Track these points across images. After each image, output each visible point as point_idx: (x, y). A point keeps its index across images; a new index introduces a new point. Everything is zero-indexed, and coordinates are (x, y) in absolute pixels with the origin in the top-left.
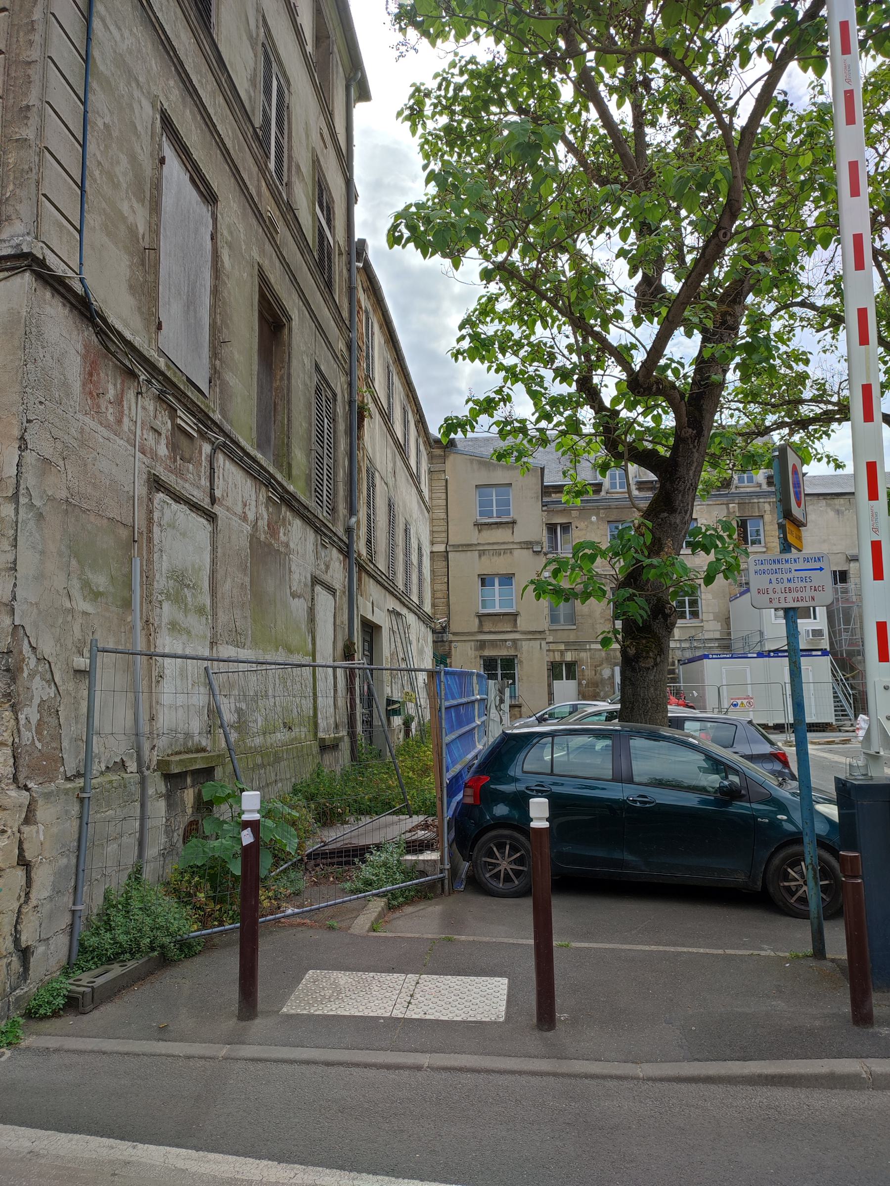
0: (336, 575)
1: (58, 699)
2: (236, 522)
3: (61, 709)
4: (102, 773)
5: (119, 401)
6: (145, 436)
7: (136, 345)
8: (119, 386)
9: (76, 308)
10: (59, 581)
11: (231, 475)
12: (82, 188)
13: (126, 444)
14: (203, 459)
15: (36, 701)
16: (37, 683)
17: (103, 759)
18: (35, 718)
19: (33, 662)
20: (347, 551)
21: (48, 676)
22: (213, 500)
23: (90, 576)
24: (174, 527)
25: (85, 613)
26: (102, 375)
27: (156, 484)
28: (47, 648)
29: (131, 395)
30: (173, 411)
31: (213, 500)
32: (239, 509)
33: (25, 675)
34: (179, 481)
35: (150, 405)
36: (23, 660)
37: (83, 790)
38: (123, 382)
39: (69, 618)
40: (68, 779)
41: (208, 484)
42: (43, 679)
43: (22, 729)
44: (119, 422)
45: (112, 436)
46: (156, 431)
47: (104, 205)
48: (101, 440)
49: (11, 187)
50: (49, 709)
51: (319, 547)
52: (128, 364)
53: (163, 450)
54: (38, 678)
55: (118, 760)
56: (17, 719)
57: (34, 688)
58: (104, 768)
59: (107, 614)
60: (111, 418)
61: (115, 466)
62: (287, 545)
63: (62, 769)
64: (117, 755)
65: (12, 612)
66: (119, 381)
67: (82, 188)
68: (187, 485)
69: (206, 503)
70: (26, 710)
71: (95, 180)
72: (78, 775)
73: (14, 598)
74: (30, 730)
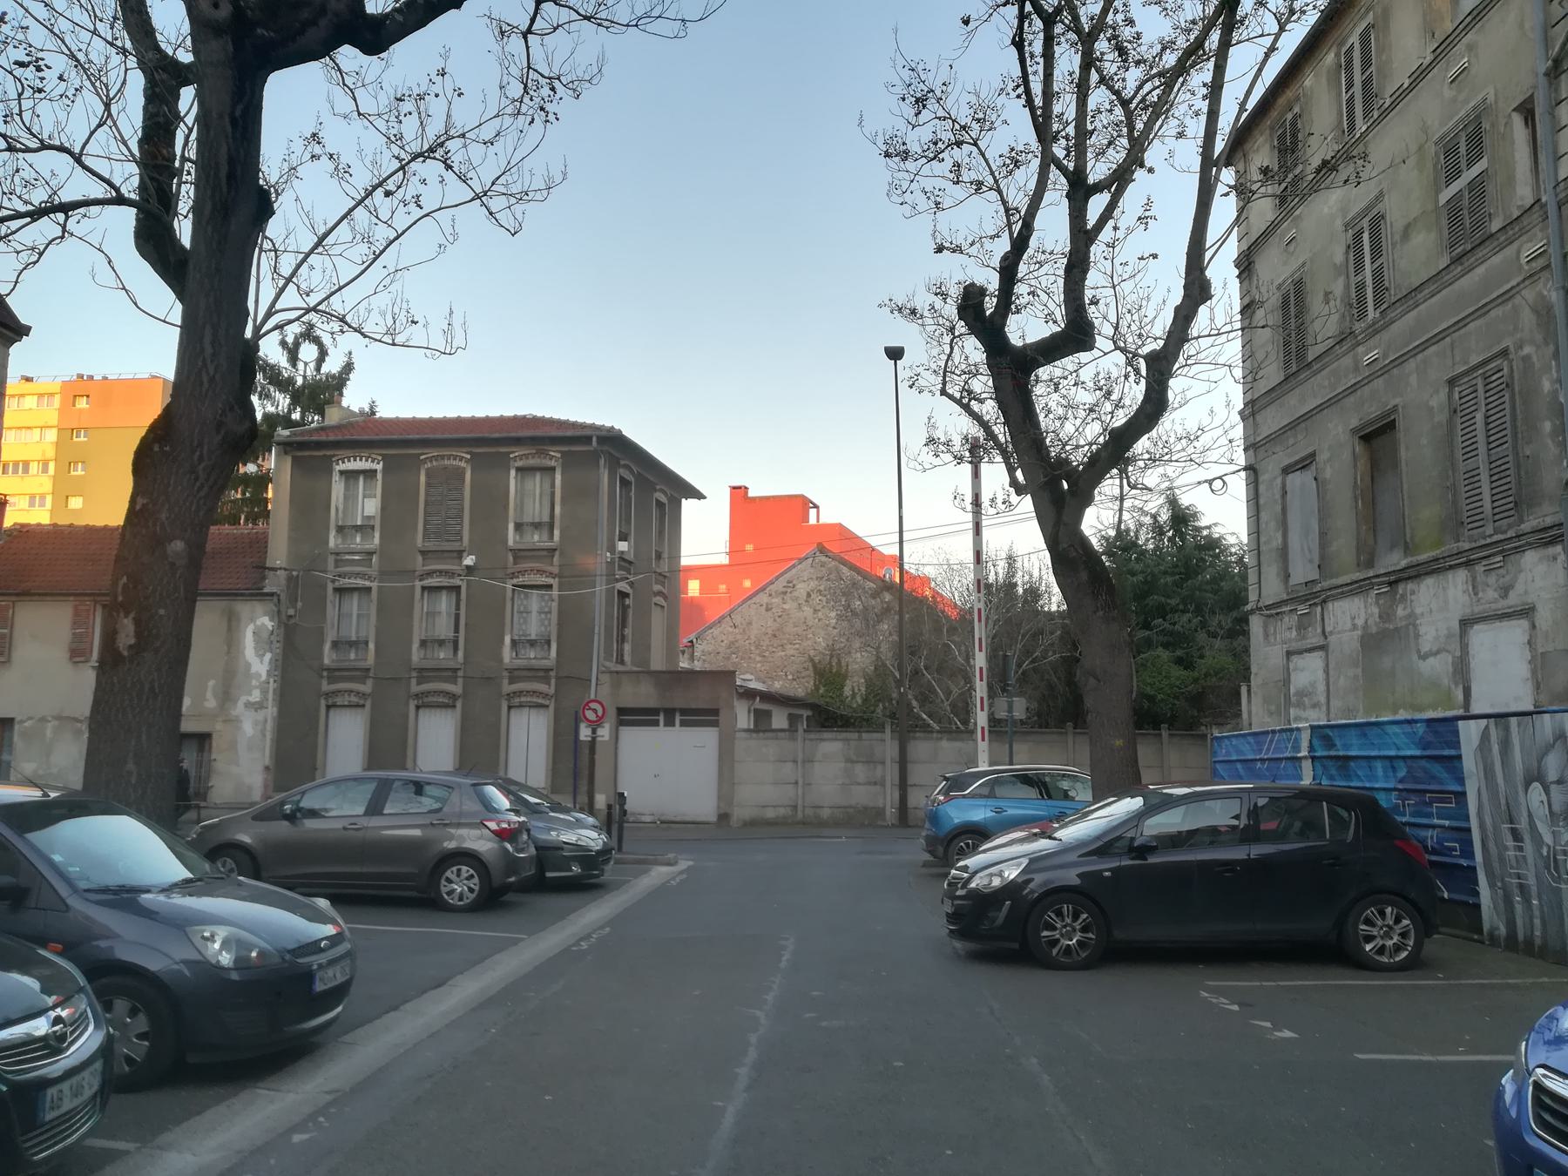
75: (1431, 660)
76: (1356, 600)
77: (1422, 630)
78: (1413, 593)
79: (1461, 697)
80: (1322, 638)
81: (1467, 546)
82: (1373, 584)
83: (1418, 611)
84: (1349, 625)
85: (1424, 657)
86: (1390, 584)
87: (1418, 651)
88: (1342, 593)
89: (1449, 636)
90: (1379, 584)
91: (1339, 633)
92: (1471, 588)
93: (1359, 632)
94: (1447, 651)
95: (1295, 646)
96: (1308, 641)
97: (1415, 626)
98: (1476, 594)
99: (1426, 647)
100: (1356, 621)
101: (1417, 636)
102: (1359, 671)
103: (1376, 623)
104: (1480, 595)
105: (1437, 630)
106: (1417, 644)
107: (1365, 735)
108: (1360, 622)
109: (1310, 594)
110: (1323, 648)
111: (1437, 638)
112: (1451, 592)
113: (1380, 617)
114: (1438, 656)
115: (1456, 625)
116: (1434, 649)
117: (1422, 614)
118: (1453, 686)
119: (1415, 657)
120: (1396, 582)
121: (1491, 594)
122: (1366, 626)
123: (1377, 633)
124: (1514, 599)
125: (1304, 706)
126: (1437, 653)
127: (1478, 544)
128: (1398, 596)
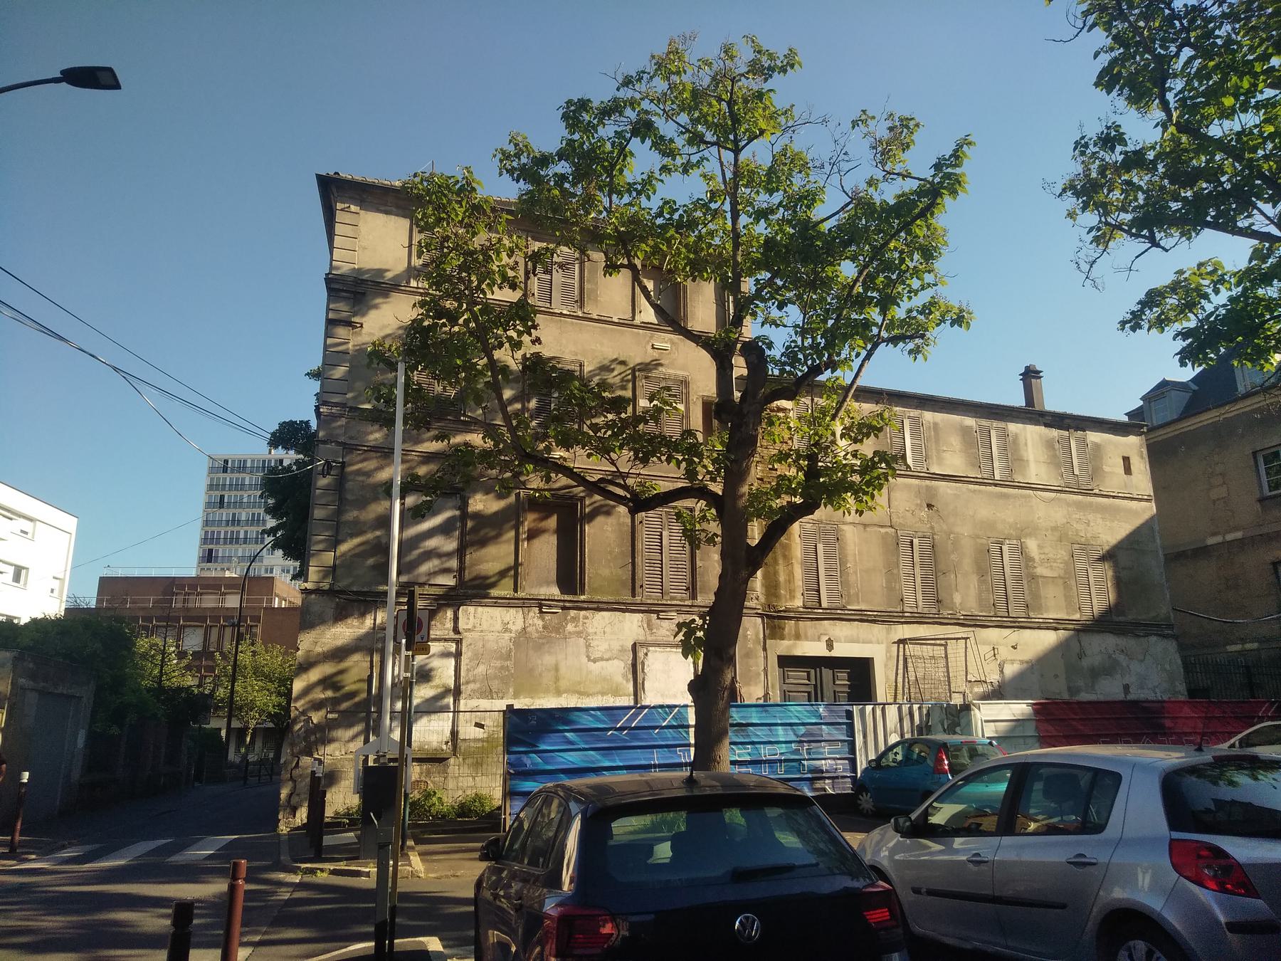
76: (512, 611)
78: (587, 618)
81: (649, 602)
82: (541, 604)
83: (591, 630)
84: (499, 627)
91: (482, 631)
92: (645, 626)
93: (513, 635)
103: (537, 631)
104: (655, 630)
107: (766, 711)
114: (610, 662)
120: (569, 608)
127: (660, 602)
128: (569, 617)
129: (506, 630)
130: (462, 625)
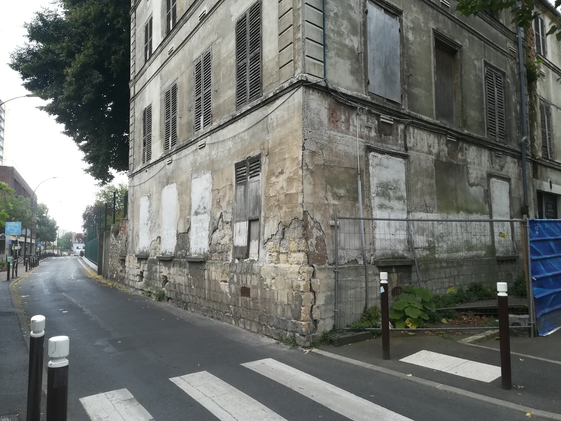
0: (511, 170)
1: (324, 236)
2: (423, 156)
3: (325, 240)
4: (346, 264)
5: (347, 121)
6: (362, 130)
7: (354, 95)
8: (347, 115)
9: (324, 91)
10: (322, 194)
11: (419, 136)
12: (324, 45)
13: (352, 137)
14: (399, 132)
15: (315, 237)
16: (315, 230)
17: (346, 258)
18: (314, 242)
19: (312, 223)
20: (518, 156)
21: (319, 228)
22: (406, 149)
23: (336, 190)
24: (380, 165)
25: (334, 204)
26: (338, 113)
27: (369, 149)
28: (318, 217)
29: (354, 116)
30: (378, 117)
31: (406, 149)
32: (426, 149)
33: (310, 227)
34: (384, 145)
35: (364, 118)
36: (308, 223)
37: (335, 269)
38: (349, 113)
39: (327, 207)
40: (330, 265)
41: (403, 142)
42: (317, 229)
43: (310, 246)
44: (348, 129)
45: (345, 135)
46: (368, 127)
47: (336, 45)
48: (339, 138)
49: (297, 57)
50: (320, 240)
51: (494, 158)
52: (349, 104)
53: (373, 134)
54: (315, 228)
55: (353, 259)
56: (307, 242)
57: (313, 232)
58: (347, 262)
59: (346, 204)
60: (343, 128)
61: (346, 146)
62: (465, 160)
63: (327, 261)
64: (353, 257)
65: (303, 207)
66: (347, 113)
67: (324, 45)
68: (389, 146)
69: (402, 152)
70: (311, 240)
71: (331, 38)
72: (334, 263)
73: (303, 202)
74: (313, 246)
75: (474, 188)
77: (471, 171)
79: (488, 210)
80: (403, 149)
83: (469, 160)
85: (472, 185)
86: (458, 139)
87: (469, 181)
88: (425, 126)
89: (482, 179)
90: (451, 135)
91: (417, 151)
94: (481, 185)
95: (373, 144)
96: (389, 146)
97: (467, 168)
98: (492, 164)
99: (472, 181)
100: (432, 148)
101: (468, 173)
102: (433, 182)
104: (494, 165)
105: (477, 173)
106: (468, 177)
108: (435, 150)
109: (396, 111)
110: (405, 157)
111: (477, 177)
112: (483, 158)
113: (449, 154)
114: (478, 187)
115: (485, 175)
116: (476, 183)
117: (470, 162)
118: (484, 203)
119: (467, 184)
121: (497, 167)
122: (438, 155)
123: (446, 163)
124: (504, 172)
125: (389, 197)
126: (477, 185)
129: (430, 153)
130: (409, 145)
